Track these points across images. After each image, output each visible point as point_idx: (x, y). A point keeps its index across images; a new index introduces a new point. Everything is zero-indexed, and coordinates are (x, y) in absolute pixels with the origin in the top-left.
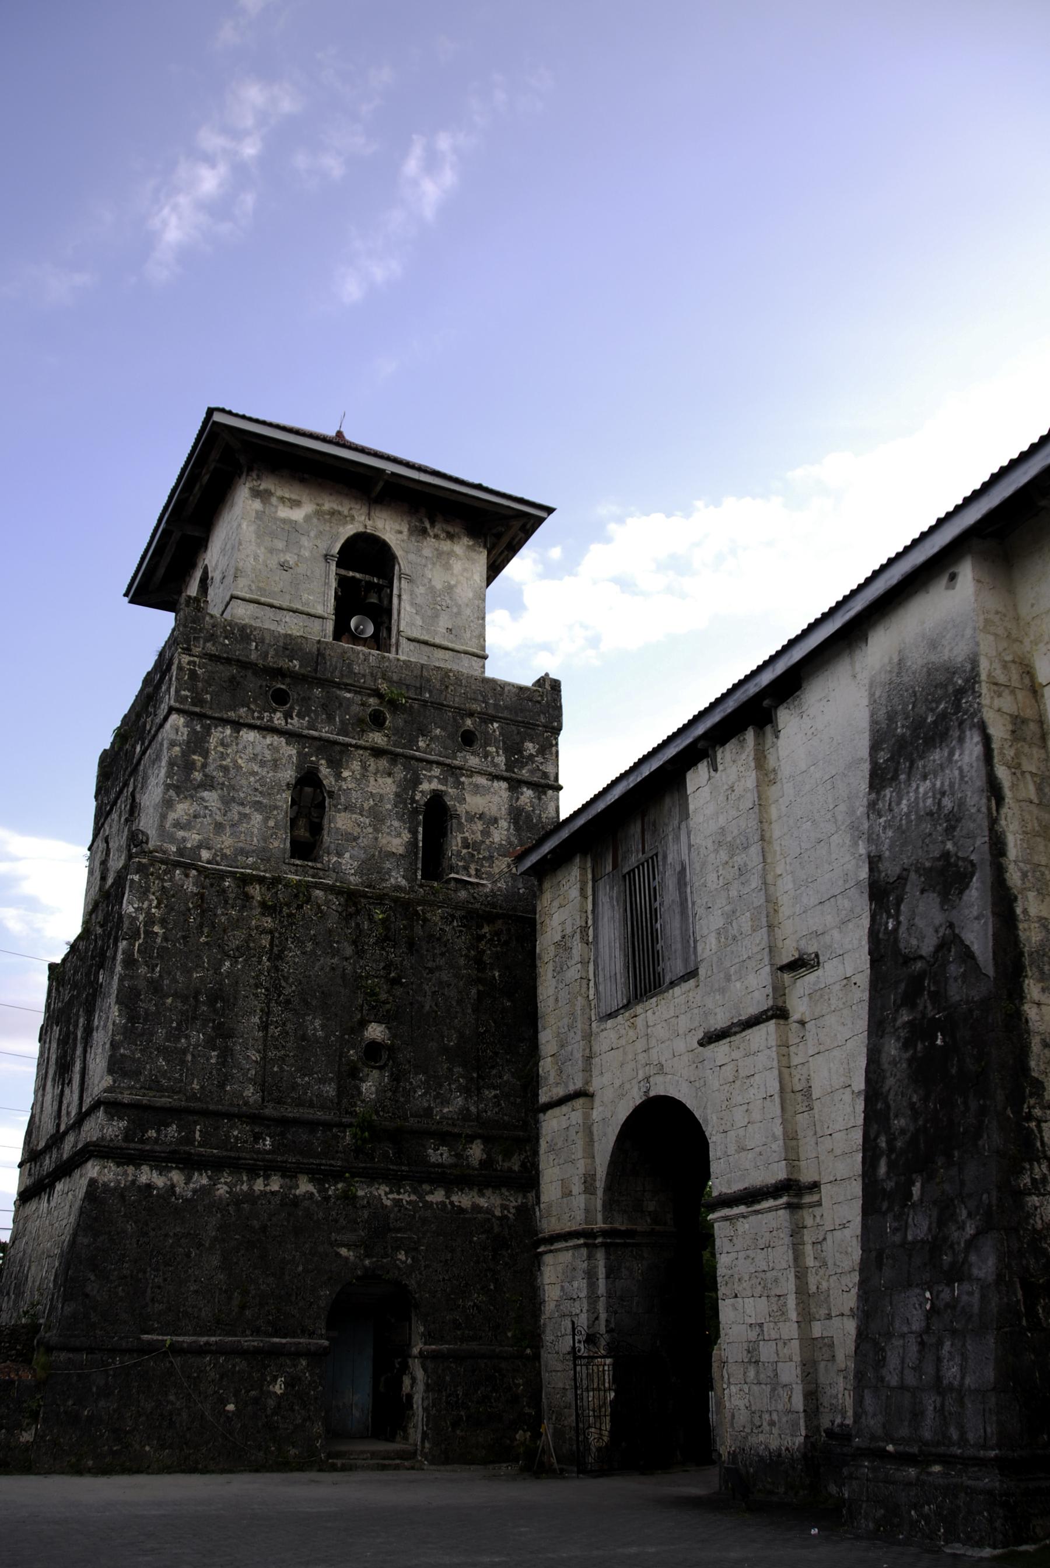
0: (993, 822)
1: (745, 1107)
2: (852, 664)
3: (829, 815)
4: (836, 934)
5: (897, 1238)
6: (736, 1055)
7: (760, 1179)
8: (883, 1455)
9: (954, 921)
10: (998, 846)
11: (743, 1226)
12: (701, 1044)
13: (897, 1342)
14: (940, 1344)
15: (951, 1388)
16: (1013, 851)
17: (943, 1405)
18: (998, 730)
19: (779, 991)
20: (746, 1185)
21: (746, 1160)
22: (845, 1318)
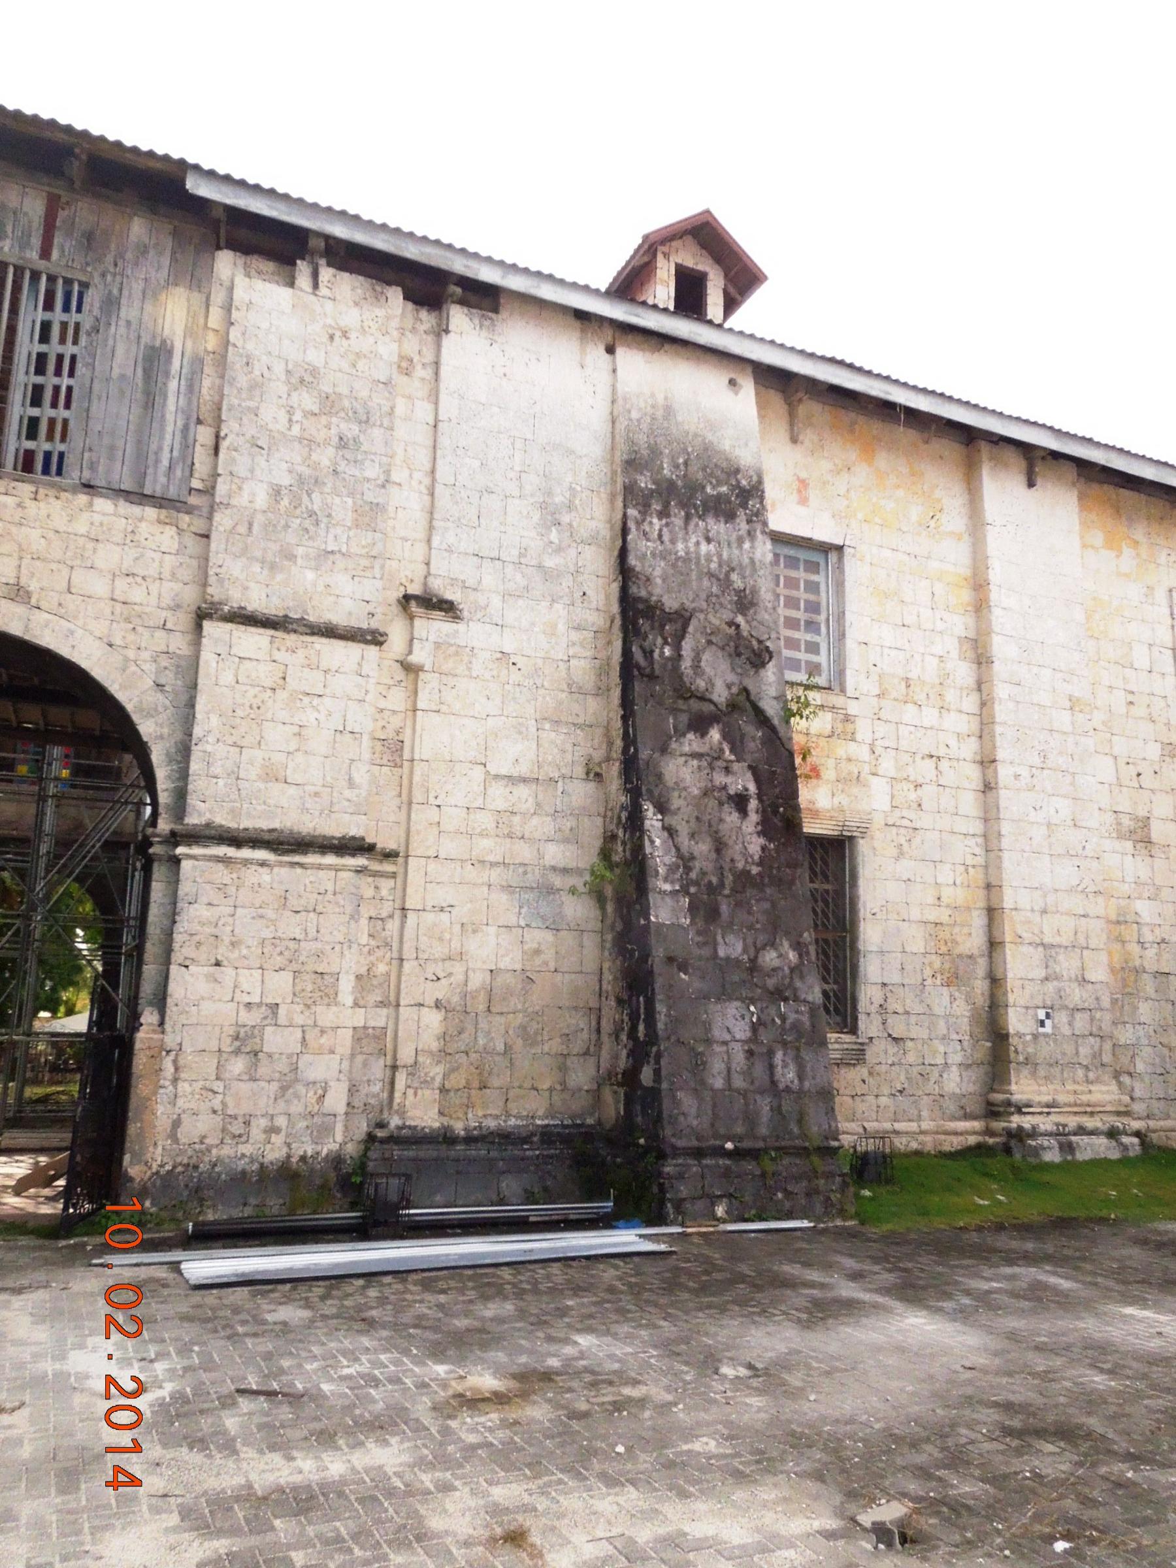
1: (296, 729)
2: (583, 351)
4: (496, 601)
5: (706, 952)
7: (311, 825)
8: (721, 1152)
9: (750, 688)
11: (253, 875)
13: (718, 1048)
14: (771, 1053)
15: (787, 1089)
17: (780, 1106)
20: (276, 825)
21: (277, 794)
22: (425, 1010)
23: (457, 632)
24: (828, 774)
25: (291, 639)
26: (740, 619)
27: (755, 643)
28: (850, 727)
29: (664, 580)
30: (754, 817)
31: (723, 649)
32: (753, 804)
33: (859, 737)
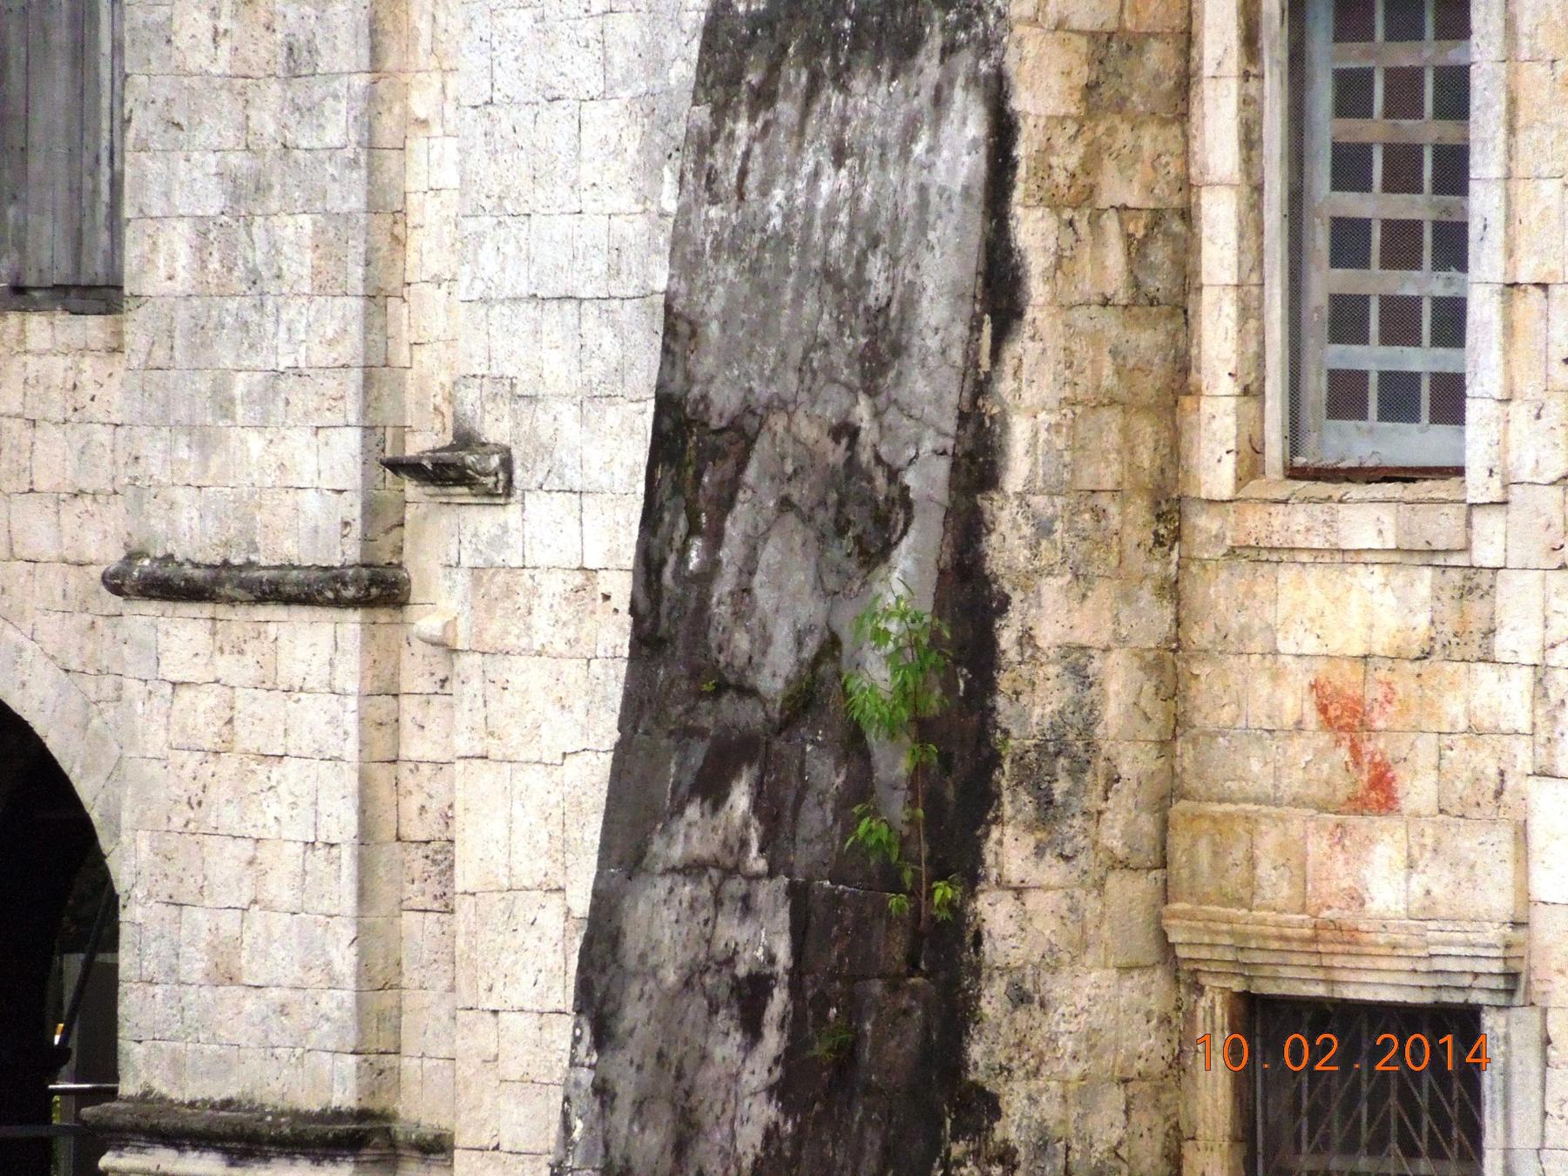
0: (981, 387)
3: (589, 29)
6: (225, 665)
7: (276, 1086)
10: (977, 463)
12: (115, 584)
16: (1018, 471)
18: (1041, 96)
19: (379, 516)
23: (505, 529)
24: (1418, 790)
25: (240, 619)
26: (862, 412)
27: (880, 481)
28: (1477, 608)
29: (724, 326)
30: (772, 1041)
31: (807, 519)
32: (778, 1002)
33: (1503, 644)
